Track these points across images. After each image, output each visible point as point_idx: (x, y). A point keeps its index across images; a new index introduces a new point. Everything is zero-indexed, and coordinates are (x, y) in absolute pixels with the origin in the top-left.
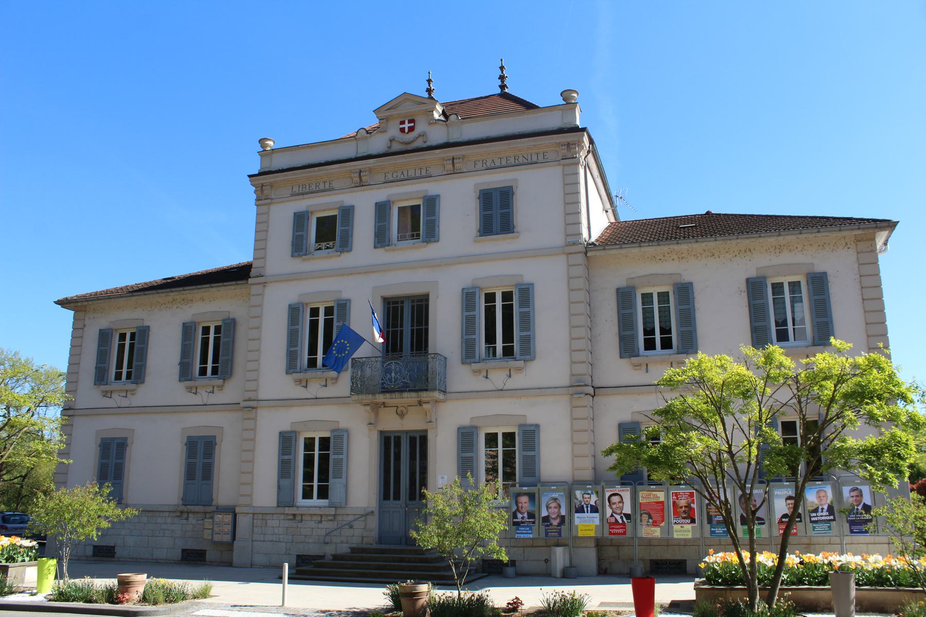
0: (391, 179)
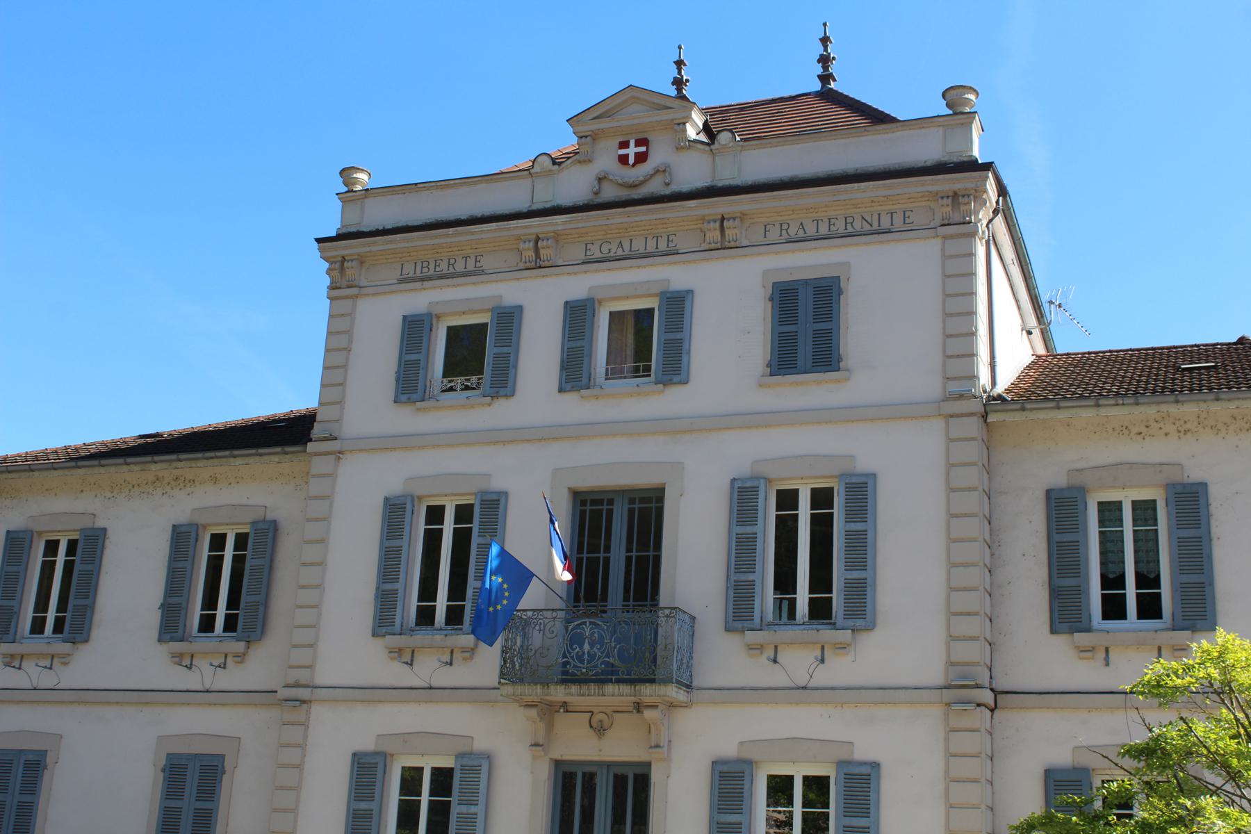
0: (598, 255)
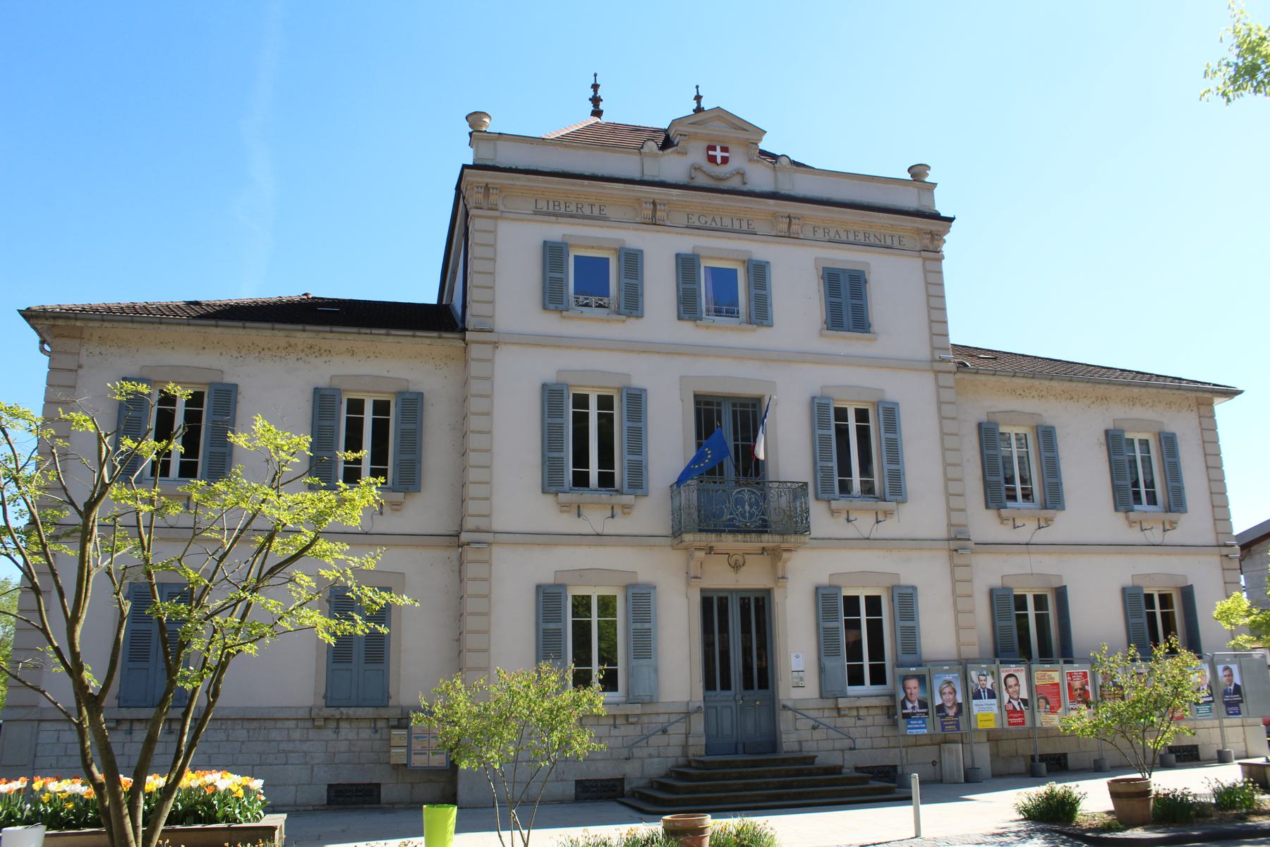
0: (697, 224)
